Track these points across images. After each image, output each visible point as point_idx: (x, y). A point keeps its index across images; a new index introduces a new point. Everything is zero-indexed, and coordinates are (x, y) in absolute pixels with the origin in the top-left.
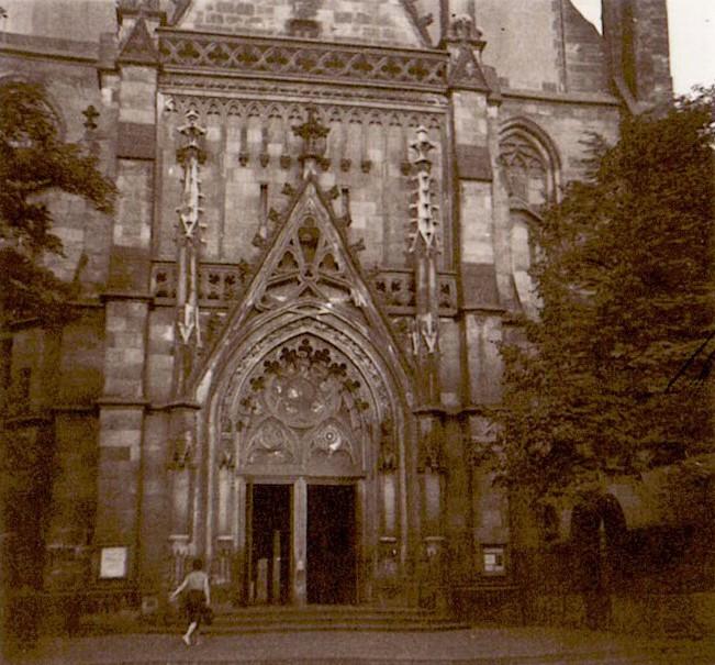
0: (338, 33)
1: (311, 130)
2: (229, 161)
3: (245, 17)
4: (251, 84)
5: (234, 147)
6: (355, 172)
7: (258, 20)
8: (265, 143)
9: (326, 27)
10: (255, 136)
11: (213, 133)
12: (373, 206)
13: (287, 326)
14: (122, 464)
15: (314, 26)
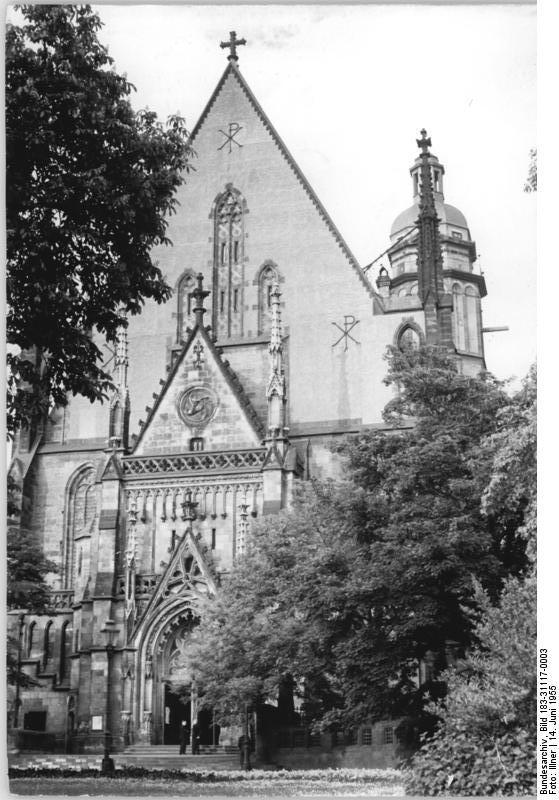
0: (214, 442)
1: (190, 505)
2: (158, 520)
3: (168, 441)
4: (165, 481)
5: (159, 513)
6: (219, 519)
7: (173, 442)
8: (174, 512)
9: (208, 440)
10: (169, 507)
11: (149, 508)
12: (227, 536)
13: (177, 607)
14: (101, 677)
15: (201, 439)
